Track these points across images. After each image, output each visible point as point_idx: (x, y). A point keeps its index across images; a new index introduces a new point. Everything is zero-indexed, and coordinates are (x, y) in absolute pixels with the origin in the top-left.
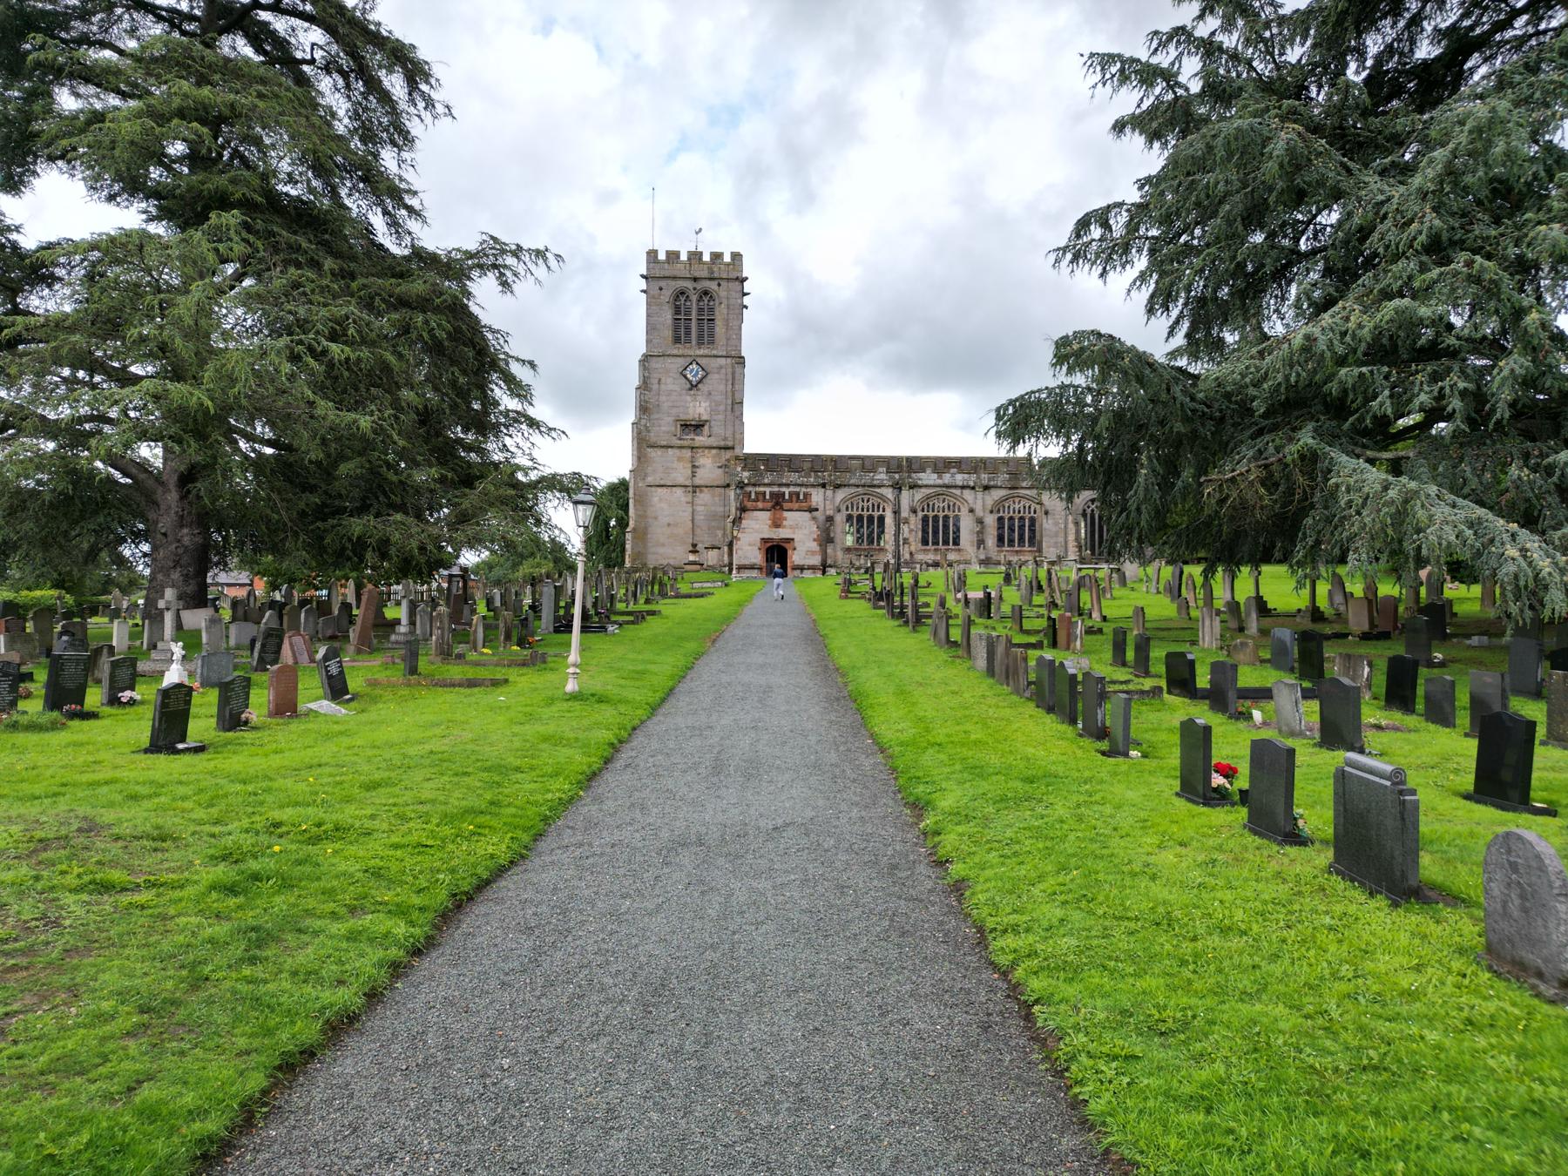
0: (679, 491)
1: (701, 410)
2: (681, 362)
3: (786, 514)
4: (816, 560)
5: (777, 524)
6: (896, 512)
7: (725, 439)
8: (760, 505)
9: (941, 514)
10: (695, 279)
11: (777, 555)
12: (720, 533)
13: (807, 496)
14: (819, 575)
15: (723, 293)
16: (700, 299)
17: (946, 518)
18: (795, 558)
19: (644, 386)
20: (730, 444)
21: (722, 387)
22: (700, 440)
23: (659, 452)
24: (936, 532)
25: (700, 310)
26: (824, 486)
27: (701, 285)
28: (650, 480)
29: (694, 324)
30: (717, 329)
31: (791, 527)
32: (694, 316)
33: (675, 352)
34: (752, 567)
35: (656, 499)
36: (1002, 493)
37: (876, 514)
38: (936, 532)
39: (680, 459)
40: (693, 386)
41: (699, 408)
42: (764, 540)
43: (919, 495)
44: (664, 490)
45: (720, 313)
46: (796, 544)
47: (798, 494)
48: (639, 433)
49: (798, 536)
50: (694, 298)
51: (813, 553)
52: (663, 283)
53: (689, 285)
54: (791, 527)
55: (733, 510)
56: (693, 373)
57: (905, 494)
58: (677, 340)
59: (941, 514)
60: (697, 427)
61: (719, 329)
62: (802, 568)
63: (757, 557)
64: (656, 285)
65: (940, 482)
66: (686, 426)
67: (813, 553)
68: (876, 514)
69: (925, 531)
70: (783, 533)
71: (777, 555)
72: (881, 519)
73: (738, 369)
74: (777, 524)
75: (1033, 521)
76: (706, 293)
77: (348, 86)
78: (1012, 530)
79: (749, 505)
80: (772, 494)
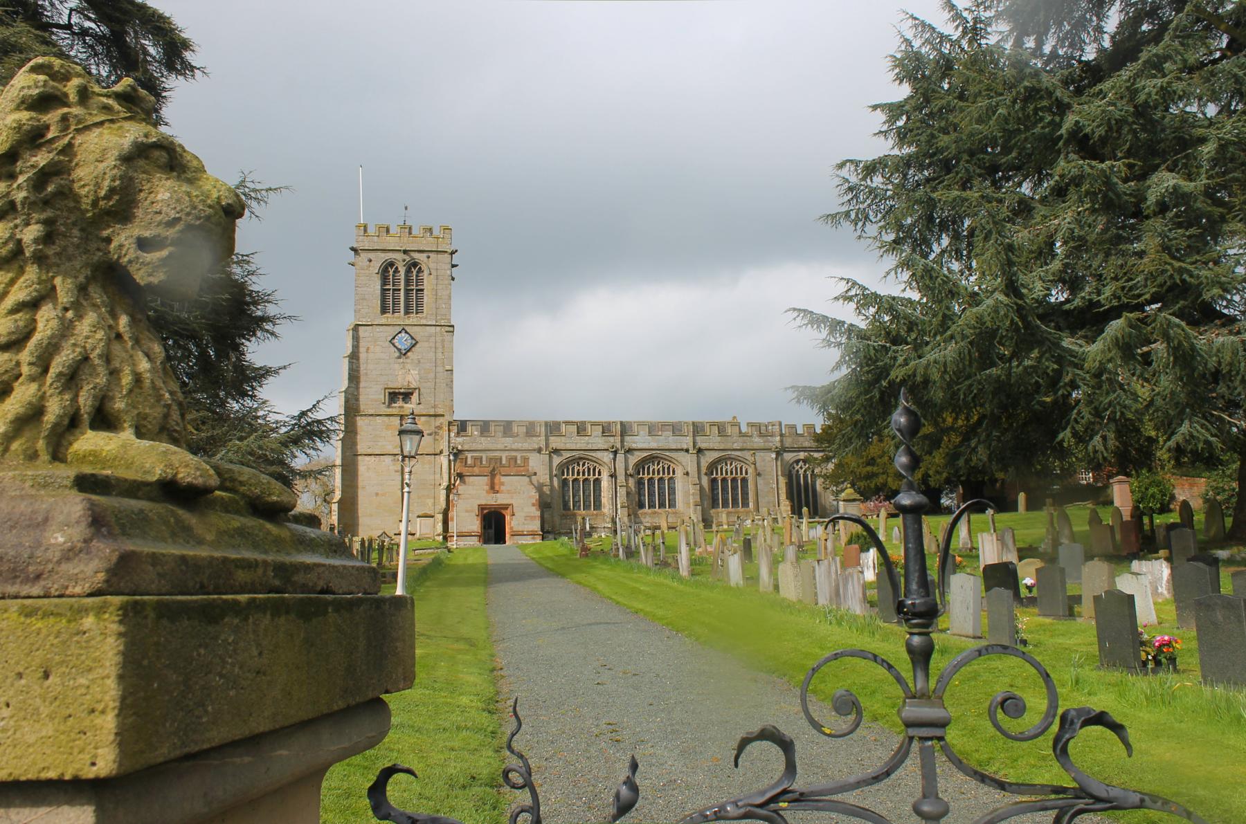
0: (388, 459)
1: (410, 378)
2: (393, 331)
3: (504, 479)
4: (536, 526)
6: (613, 476)
7: (435, 407)
8: (476, 470)
9: (656, 477)
10: (405, 252)
12: (430, 502)
13: (526, 460)
14: (538, 540)
15: (432, 265)
16: (408, 271)
17: (661, 479)
18: (512, 523)
19: (354, 357)
20: (440, 411)
21: (432, 355)
22: (409, 407)
23: (367, 420)
24: (651, 494)
25: (408, 282)
26: (539, 450)
27: (407, 258)
29: (402, 292)
30: (425, 300)
31: (509, 492)
32: (402, 287)
33: (383, 321)
36: (716, 455)
37: (592, 478)
38: (651, 494)
39: (388, 427)
40: (404, 354)
41: (406, 376)
42: (482, 508)
43: (634, 459)
45: (428, 283)
47: (515, 459)
48: (347, 401)
49: (515, 501)
50: (402, 271)
52: (371, 255)
53: (399, 256)
54: (509, 492)
55: (446, 476)
56: (403, 341)
57: (620, 457)
58: (384, 310)
59: (656, 477)
60: (407, 396)
61: (427, 298)
63: (475, 525)
64: (364, 256)
65: (654, 445)
66: (394, 396)
67: (533, 518)
68: (592, 478)
69: (640, 493)
70: (500, 499)
71: (494, 525)
72: (597, 482)
73: (447, 337)
74: (493, 488)
75: (744, 480)
76: (415, 264)
77: (109, 51)
78: (724, 489)
79: (465, 471)
80: (490, 460)
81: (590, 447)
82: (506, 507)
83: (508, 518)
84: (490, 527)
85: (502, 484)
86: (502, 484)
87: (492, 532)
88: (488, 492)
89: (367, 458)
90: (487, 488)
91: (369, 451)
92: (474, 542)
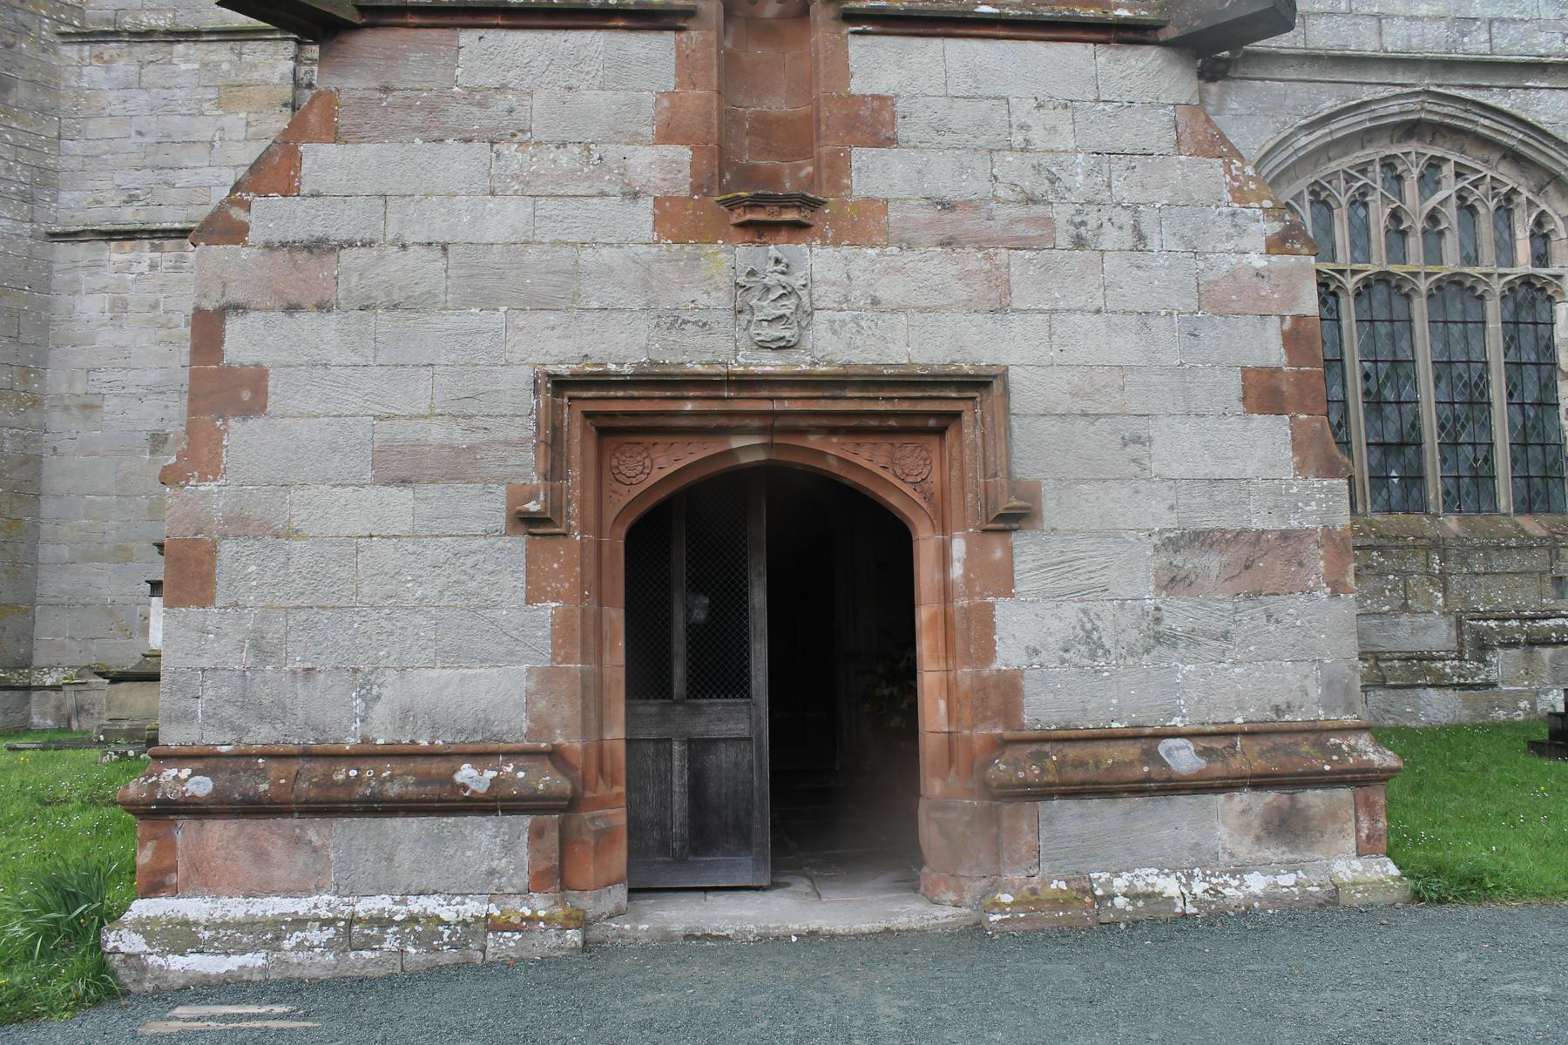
5: (762, 191)
11: (772, 605)
18: (1037, 624)
23: (125, 60)
28: (76, 204)
31: (951, 223)
34: (418, 787)
35: (91, 306)
39: (230, 94)
42: (600, 411)
44: (142, 254)
46: (1035, 449)
49: (1050, 346)
51: (1259, 561)
62: (1113, 770)
63: (483, 639)
67: (1259, 561)
70: (860, 308)
81: (1476, 45)
82: (937, 405)
83: (944, 561)
84: (719, 676)
85: (875, 124)
86: (875, 124)
87: (740, 726)
88: (677, 222)
89: (115, 254)
90: (665, 166)
91: (130, 217)
92: (463, 883)
